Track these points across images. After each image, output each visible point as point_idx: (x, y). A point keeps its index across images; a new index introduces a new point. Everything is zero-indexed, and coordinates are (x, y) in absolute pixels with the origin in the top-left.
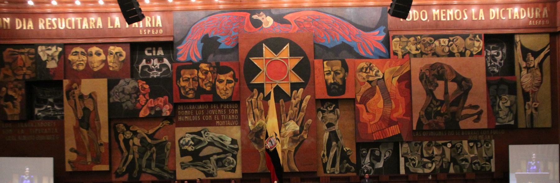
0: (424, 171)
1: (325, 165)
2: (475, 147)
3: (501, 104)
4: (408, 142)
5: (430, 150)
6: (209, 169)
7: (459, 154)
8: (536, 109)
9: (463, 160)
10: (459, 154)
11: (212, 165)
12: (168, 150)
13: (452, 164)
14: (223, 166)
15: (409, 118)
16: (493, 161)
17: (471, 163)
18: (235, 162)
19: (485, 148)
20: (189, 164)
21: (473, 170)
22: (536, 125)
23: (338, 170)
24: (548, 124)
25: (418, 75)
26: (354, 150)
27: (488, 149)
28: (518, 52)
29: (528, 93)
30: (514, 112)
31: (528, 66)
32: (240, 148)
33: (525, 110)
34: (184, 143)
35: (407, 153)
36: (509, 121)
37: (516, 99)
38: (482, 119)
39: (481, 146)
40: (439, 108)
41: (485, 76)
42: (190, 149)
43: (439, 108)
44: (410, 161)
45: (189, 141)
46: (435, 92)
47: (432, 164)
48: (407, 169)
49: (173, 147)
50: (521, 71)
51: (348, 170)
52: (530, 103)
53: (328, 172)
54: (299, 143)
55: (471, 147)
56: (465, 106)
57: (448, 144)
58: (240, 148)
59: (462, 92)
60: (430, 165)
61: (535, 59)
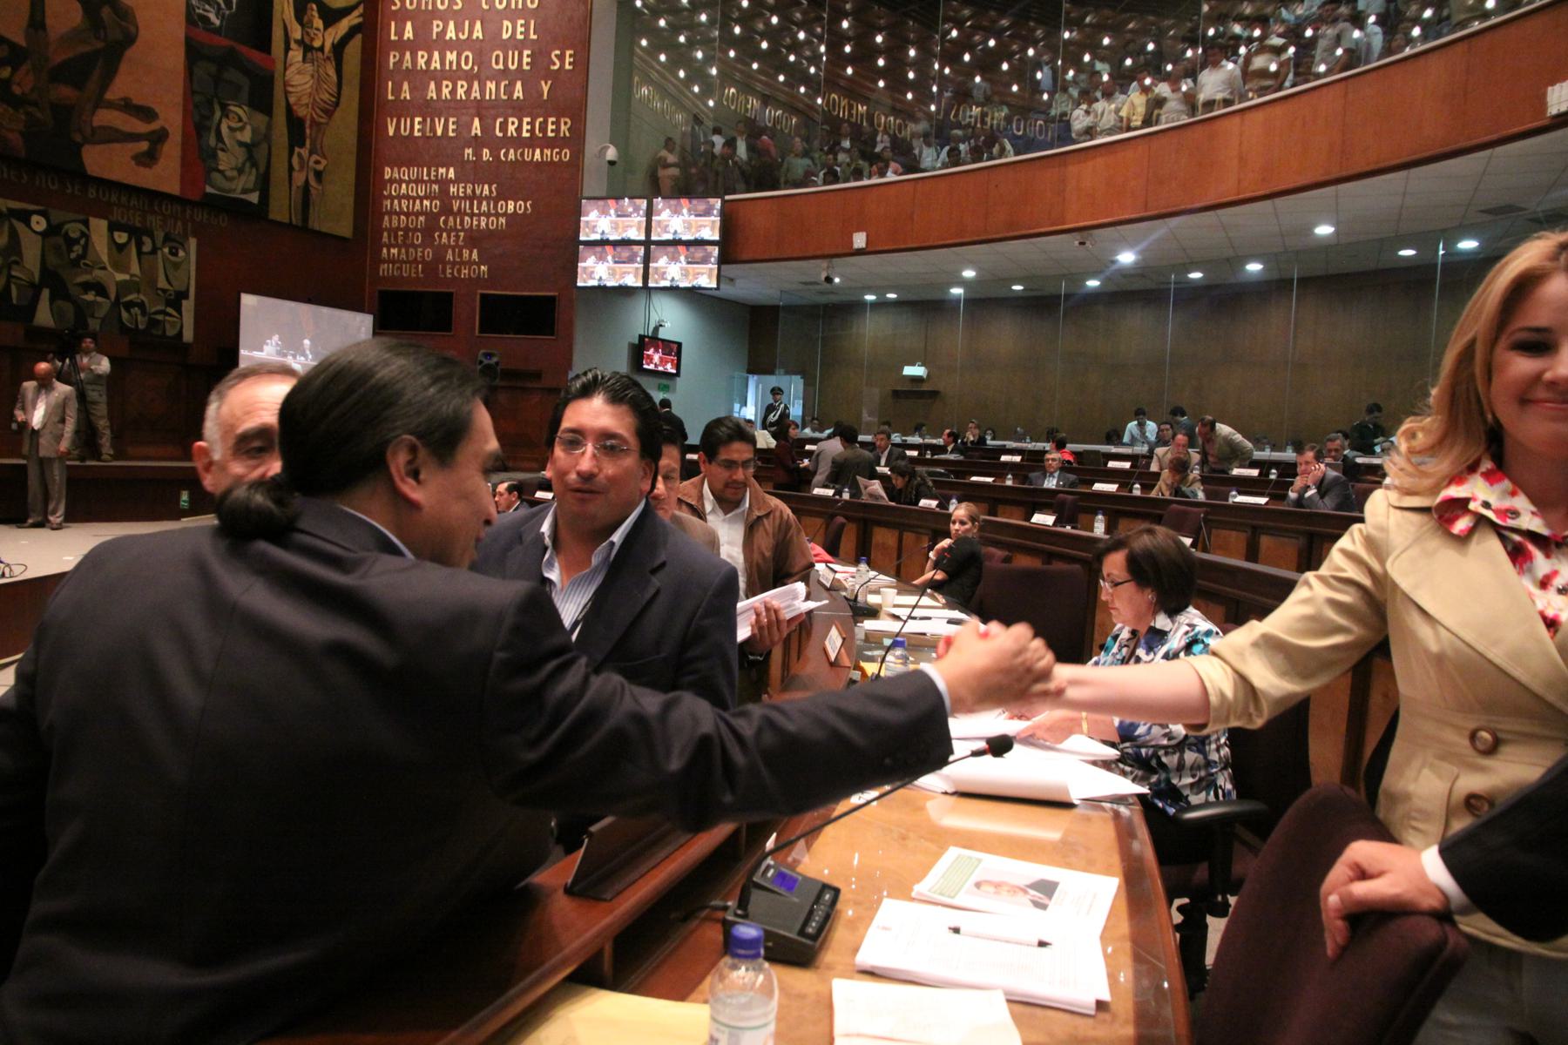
7: (75, 263)
8: (319, 175)
9: (87, 287)
10: (75, 263)
13: (46, 293)
16: (188, 306)
19: (165, 260)
22: (315, 224)
24: (345, 229)
27: (176, 266)
30: (262, 169)
31: (307, 40)
36: (245, 191)
37: (269, 127)
38: (162, 162)
39: (154, 251)
50: (287, 49)
52: (305, 152)
55: (121, 248)
56: (109, 96)
57: (35, 218)
61: (326, 28)
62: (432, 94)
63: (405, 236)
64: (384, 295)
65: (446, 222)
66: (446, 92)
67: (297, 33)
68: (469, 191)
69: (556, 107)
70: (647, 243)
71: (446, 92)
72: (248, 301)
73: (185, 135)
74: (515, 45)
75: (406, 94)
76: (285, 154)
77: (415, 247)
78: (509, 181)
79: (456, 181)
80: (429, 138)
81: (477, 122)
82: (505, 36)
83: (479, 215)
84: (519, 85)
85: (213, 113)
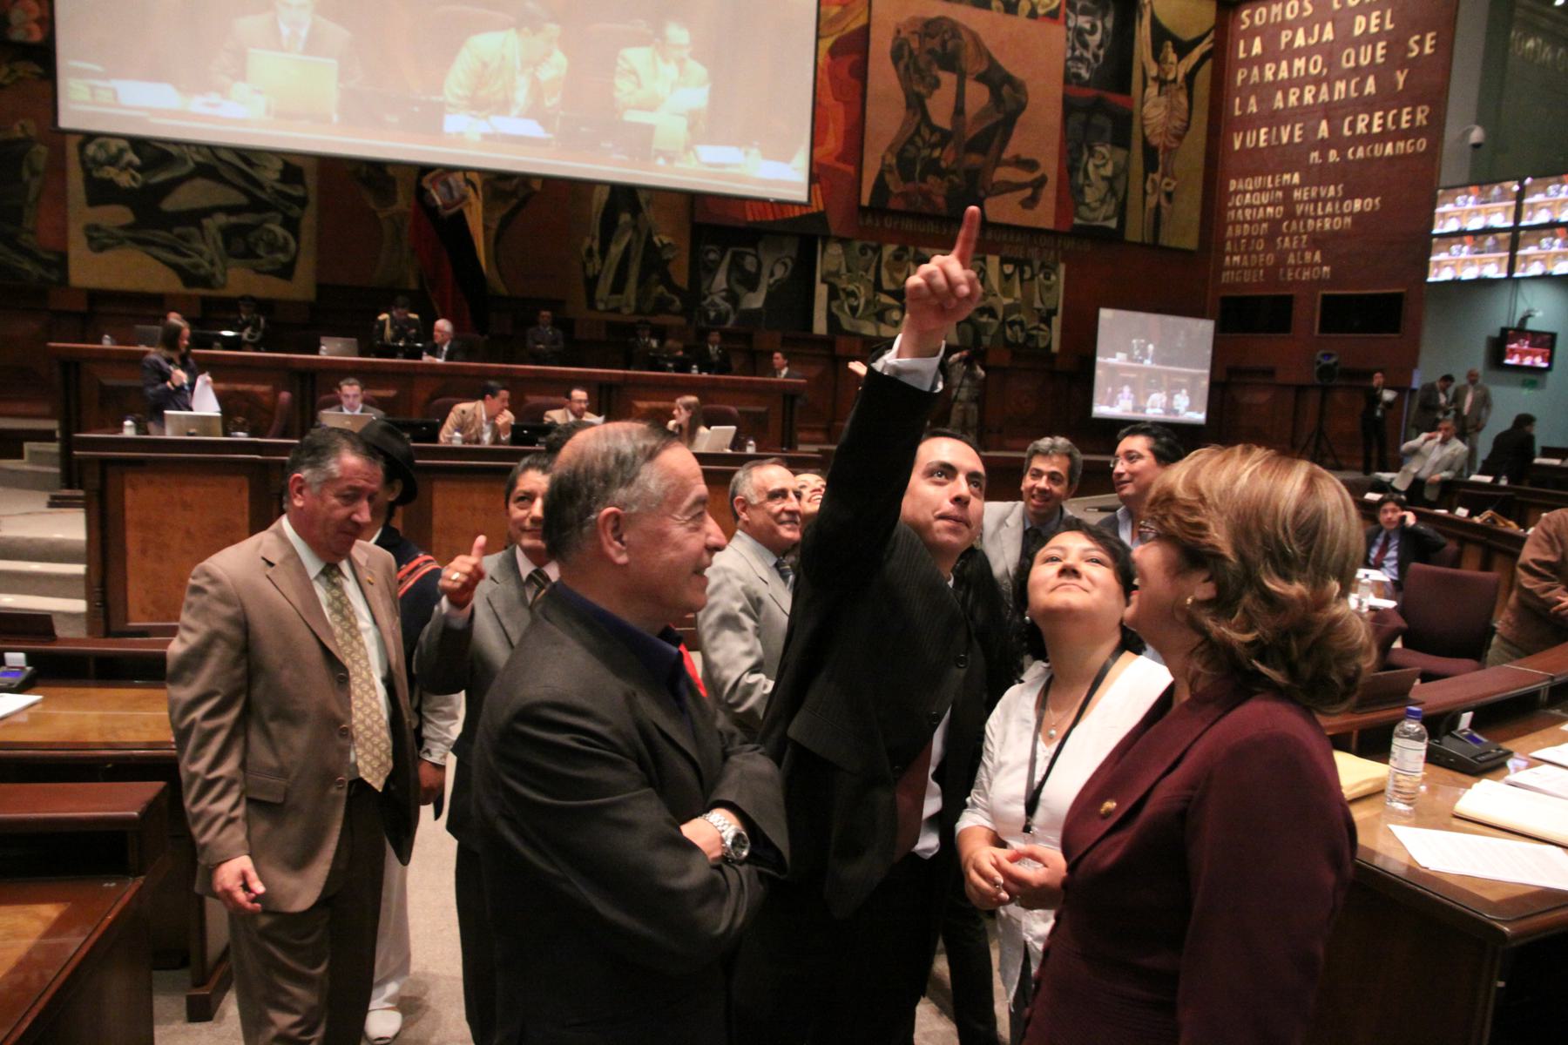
0: (878, 329)
1: (592, 283)
2: (1017, 276)
3: (1091, 168)
4: (843, 241)
5: (900, 271)
6: (196, 259)
8: (1169, 196)
11: (206, 250)
12: (34, 173)
14: (249, 254)
15: (851, 169)
16: (1056, 321)
17: (1003, 322)
18: (293, 245)
20: (121, 233)
21: (1007, 344)
22: (1164, 241)
23: (633, 303)
24: (1190, 242)
25: (887, 46)
26: (685, 245)
27: (1049, 288)
28: (1143, 32)
29: (1155, 149)
30: (1121, 195)
32: (313, 199)
33: (1145, 193)
34: (102, 156)
35: (837, 274)
36: (1106, 218)
37: (1128, 159)
38: (1042, 202)
39: (1032, 278)
40: (936, 153)
41: (1060, 80)
42: (124, 180)
43: (936, 153)
44: (842, 295)
45: (121, 151)
46: (927, 102)
47: (903, 312)
48: (832, 319)
49: (58, 167)
50: (1145, 86)
51: (662, 306)
52: (1157, 177)
53: (601, 306)
54: (514, 201)
55: (1008, 277)
56: (1005, 156)
58: (313, 199)
59: (1000, 116)
60: (896, 315)
61: (1180, 59)
62: (1279, 103)
63: (1248, 244)
64: (1224, 300)
65: (1288, 227)
66: (1293, 100)
67: (1153, 70)
68: (1313, 194)
69: (1411, 97)
70: (1515, 230)
71: (1293, 100)
72: (1105, 314)
73: (1060, 179)
74: (1369, 39)
75: (1253, 108)
76: (1140, 182)
77: (1258, 253)
78: (1354, 179)
79: (1301, 185)
80: (1274, 148)
81: (1324, 125)
82: (1358, 32)
83: (1323, 217)
84: (1371, 81)
85: (1081, 154)
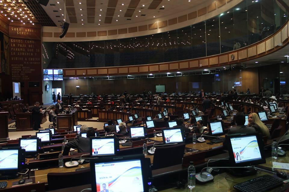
62: (19, 54)
70: (53, 75)
74: (30, 48)
81: (26, 59)
84: (32, 54)
